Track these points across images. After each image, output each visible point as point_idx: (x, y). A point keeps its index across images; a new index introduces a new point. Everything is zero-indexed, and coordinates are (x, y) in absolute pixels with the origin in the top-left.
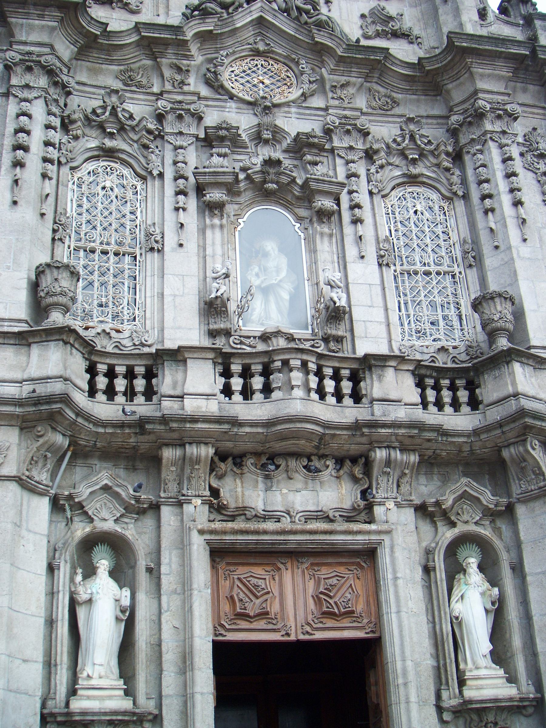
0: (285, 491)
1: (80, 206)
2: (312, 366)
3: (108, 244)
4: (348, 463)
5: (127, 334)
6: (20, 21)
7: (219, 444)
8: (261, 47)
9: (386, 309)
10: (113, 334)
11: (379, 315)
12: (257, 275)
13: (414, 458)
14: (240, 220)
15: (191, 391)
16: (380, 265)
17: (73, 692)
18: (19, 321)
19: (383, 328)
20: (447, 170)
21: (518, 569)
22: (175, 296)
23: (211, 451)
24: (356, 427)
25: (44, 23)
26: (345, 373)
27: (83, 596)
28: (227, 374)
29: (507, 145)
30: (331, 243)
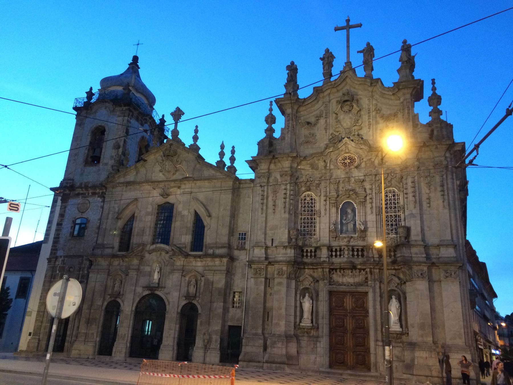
8: (347, 151)
11: (375, 230)
12: (346, 220)
16: (376, 215)
17: (300, 322)
21: (405, 298)
26: (360, 250)
27: (302, 301)
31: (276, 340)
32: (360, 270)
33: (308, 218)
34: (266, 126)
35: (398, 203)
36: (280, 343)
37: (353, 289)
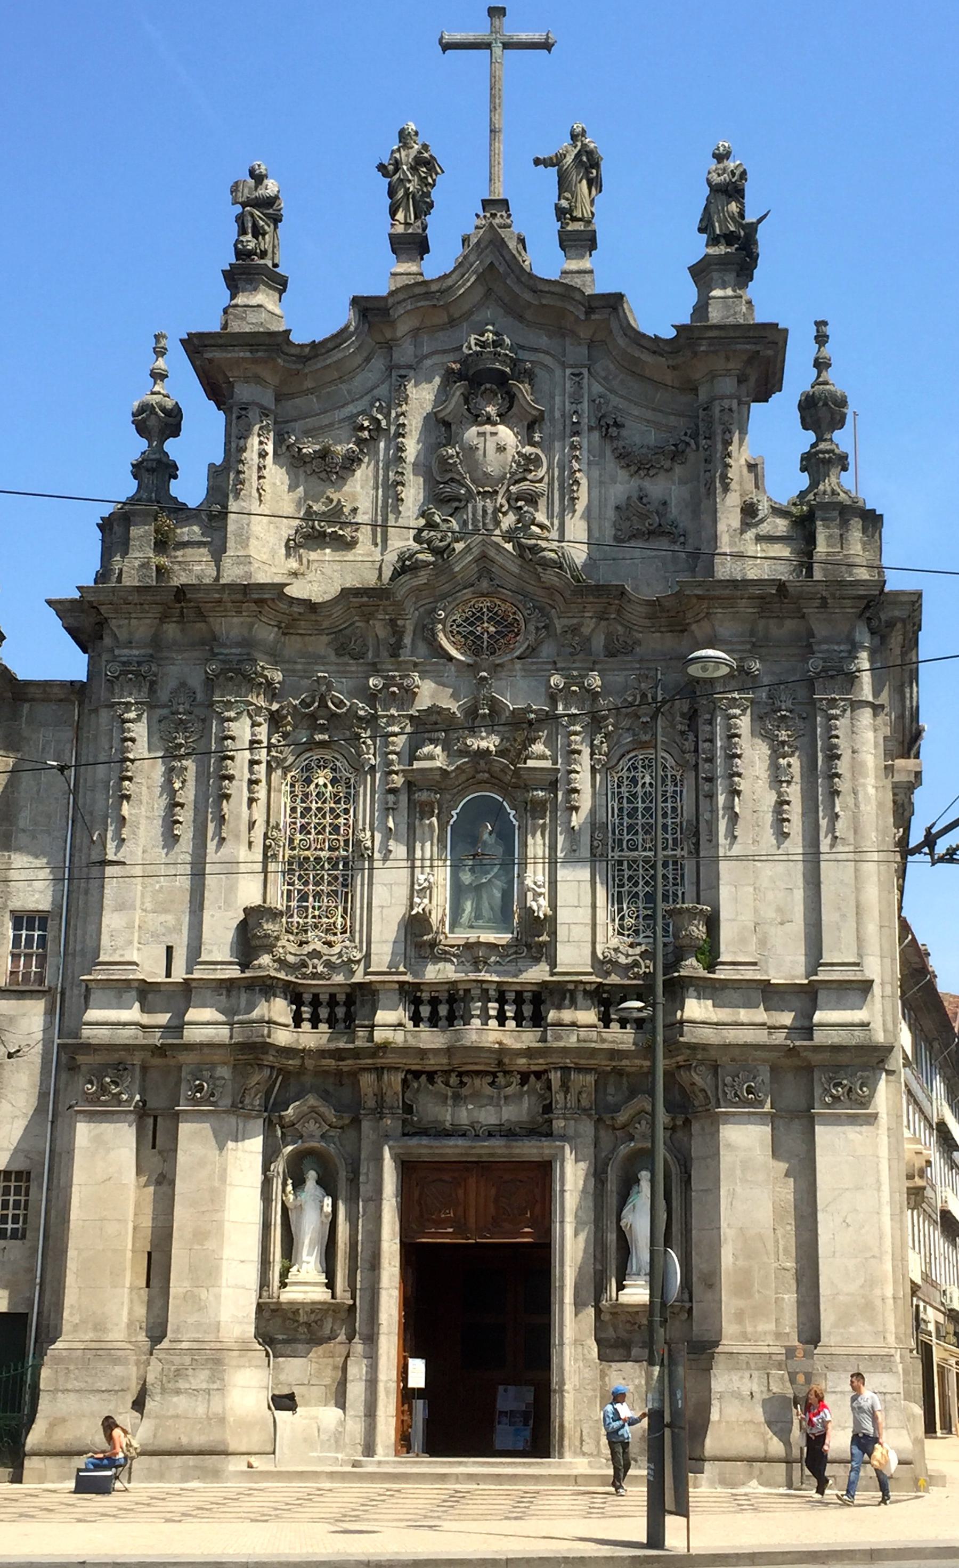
0: (470, 1107)
1: (293, 810)
2: (492, 993)
3: (321, 849)
4: (532, 1078)
5: (336, 950)
6: (219, 620)
7: (407, 1068)
9: (594, 907)
10: (325, 949)
11: (584, 915)
13: (590, 1079)
14: (453, 813)
15: (381, 1023)
18: (231, 963)
19: (588, 930)
20: (682, 733)
22: (382, 907)
23: (401, 1076)
24: (529, 1053)
25: (242, 619)
28: (417, 1002)
29: (735, 717)
30: (543, 835)
31: (187, 1360)
32: (525, 1077)
33: (318, 859)
34: (139, 446)
35: (674, 809)
36: (204, 1375)
37: (497, 1148)
